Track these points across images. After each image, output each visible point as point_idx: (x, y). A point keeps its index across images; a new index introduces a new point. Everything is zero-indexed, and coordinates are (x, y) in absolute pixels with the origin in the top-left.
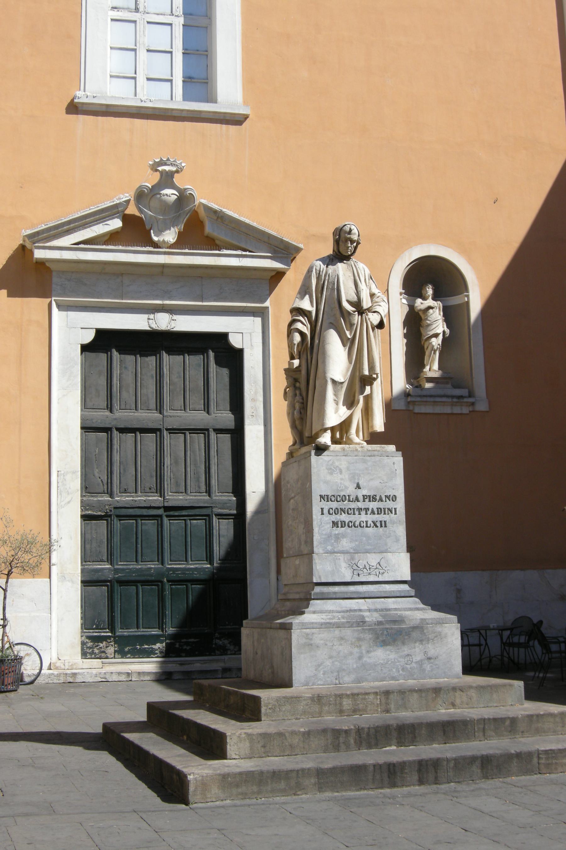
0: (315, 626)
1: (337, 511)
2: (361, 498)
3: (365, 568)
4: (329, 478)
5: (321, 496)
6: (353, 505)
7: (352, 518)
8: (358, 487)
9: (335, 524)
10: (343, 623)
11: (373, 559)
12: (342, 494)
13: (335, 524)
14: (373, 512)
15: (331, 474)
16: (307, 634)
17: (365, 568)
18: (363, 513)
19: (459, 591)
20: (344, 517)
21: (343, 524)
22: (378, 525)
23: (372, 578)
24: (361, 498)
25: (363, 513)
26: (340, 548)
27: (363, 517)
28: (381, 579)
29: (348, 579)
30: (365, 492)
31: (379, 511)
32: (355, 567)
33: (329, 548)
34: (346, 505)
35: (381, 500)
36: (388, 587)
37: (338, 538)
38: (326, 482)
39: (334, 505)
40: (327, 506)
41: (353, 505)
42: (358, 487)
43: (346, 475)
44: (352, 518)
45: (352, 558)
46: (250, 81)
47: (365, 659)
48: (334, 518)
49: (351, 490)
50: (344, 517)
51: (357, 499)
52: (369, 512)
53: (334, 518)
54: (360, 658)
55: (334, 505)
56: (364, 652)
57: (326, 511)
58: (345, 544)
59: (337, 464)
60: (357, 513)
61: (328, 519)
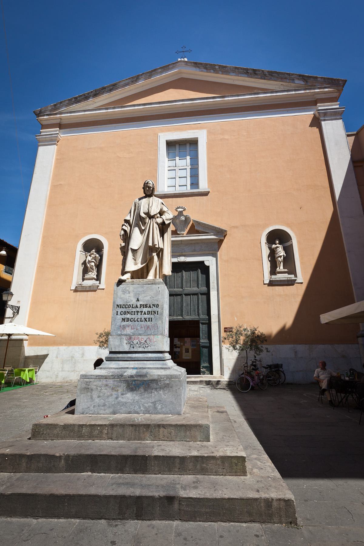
0: (93, 377)
1: (125, 313)
2: (139, 306)
3: (137, 343)
4: (122, 296)
5: (117, 305)
6: (134, 310)
7: (133, 316)
8: (138, 300)
9: (123, 320)
10: (109, 376)
11: (144, 338)
12: (128, 304)
13: (123, 320)
14: (145, 314)
15: (124, 294)
16: (87, 382)
17: (137, 343)
18: (139, 314)
19: (296, 352)
20: (128, 316)
21: (128, 320)
22: (147, 320)
23: (141, 350)
24: (139, 306)
25: (139, 314)
26: (125, 333)
27: (139, 316)
28: (146, 350)
29: (127, 350)
30: (141, 303)
31: (149, 313)
32: (132, 343)
33: (119, 332)
34: (130, 310)
35: (150, 307)
36: (150, 355)
37: (124, 327)
38: (121, 298)
39: (124, 310)
40: (120, 310)
41: (134, 310)
42: (138, 300)
43: (132, 294)
44: (133, 316)
45: (130, 338)
46: (210, 181)
47: (119, 399)
48: (123, 316)
49: (133, 301)
50: (128, 316)
51: (137, 307)
52: (143, 313)
53: (123, 316)
54: (117, 398)
55: (124, 310)
56: (120, 394)
57: (119, 313)
58: (128, 331)
59: (127, 289)
60: (136, 314)
61: (120, 317)
